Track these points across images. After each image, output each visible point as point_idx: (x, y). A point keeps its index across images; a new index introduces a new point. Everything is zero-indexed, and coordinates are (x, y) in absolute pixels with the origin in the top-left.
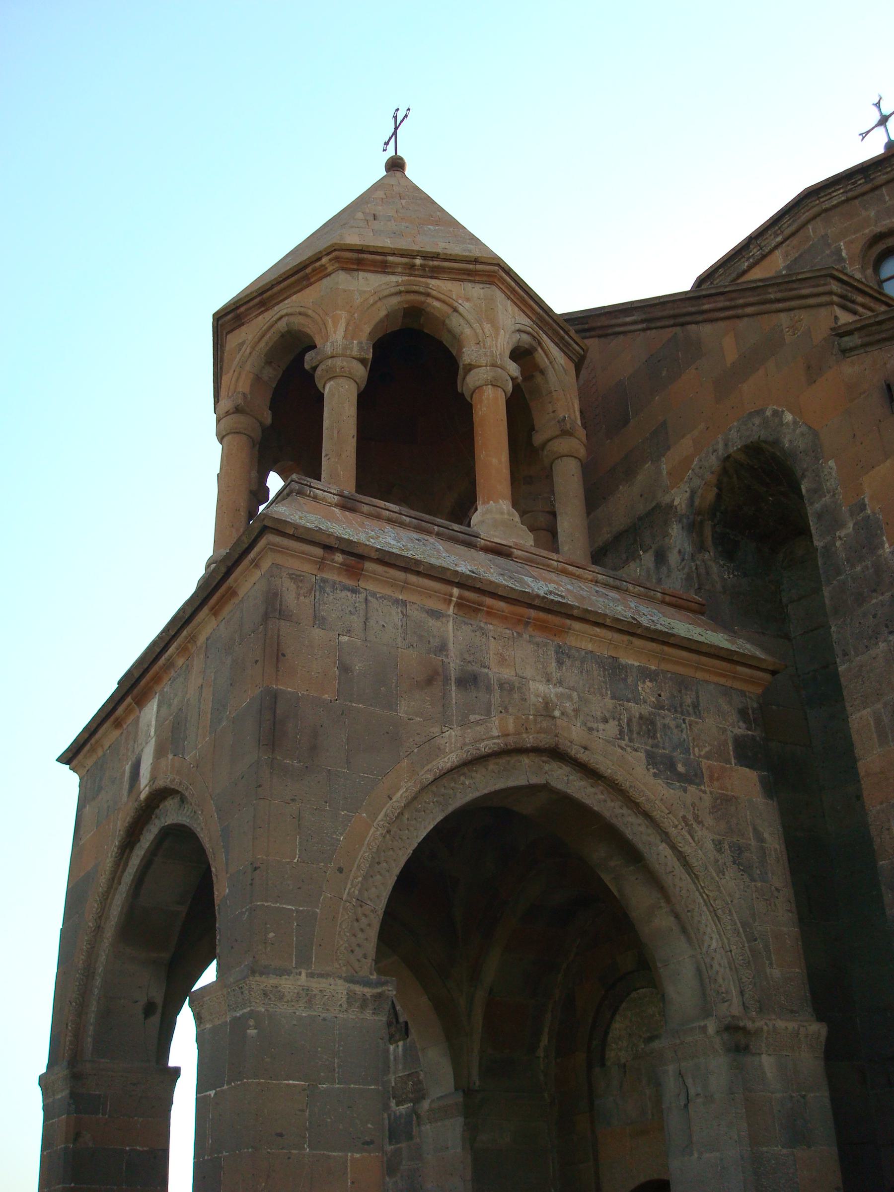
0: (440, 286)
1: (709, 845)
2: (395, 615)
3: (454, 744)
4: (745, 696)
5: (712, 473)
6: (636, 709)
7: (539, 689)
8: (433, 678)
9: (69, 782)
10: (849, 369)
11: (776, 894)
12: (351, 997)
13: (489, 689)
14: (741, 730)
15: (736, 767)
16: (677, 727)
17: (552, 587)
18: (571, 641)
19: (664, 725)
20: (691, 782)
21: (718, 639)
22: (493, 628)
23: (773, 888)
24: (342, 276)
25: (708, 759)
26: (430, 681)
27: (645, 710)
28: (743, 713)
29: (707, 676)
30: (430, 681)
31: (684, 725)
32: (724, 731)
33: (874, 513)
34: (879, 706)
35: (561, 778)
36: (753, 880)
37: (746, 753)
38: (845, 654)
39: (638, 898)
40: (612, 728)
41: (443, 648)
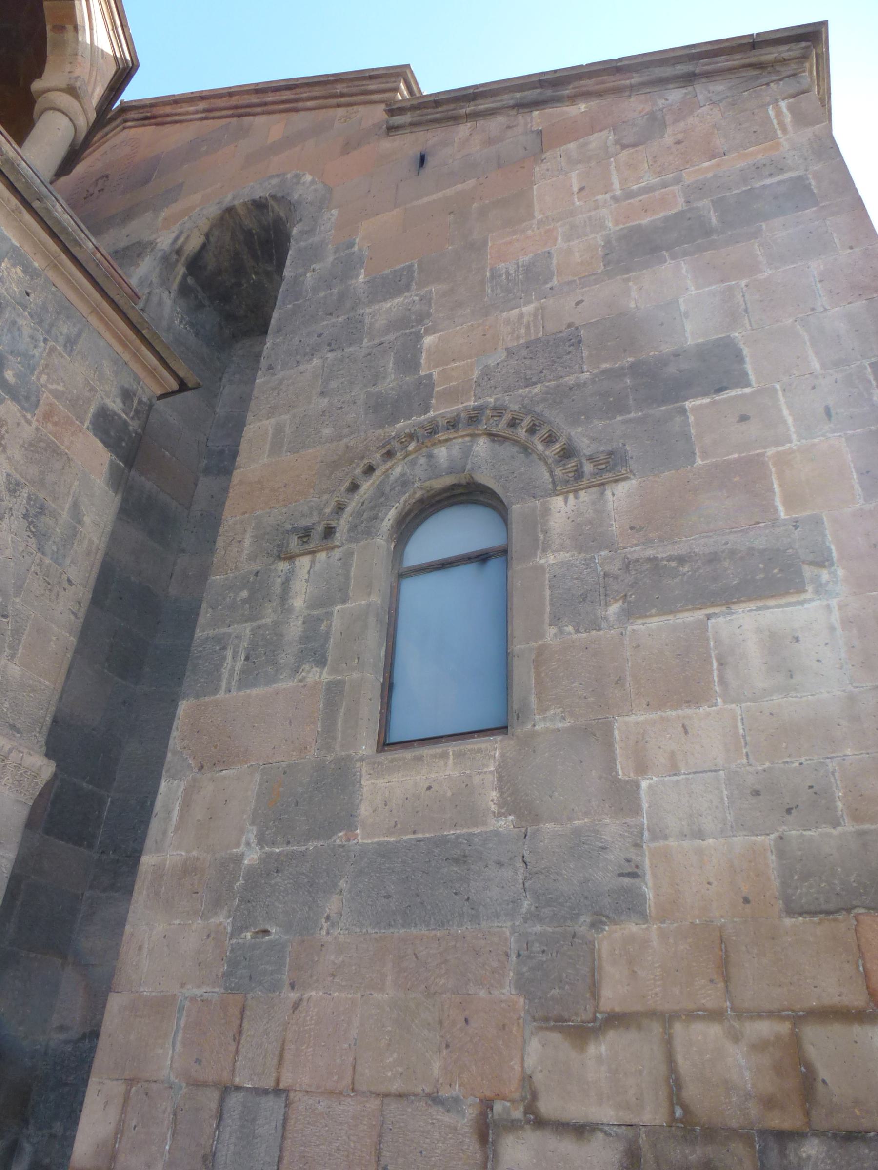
4: (139, 384)
5: (208, 219)
10: (387, 145)
11: (65, 584)
14: (115, 405)
15: (88, 432)
16: (32, 337)
19: (14, 323)
20: (15, 398)
23: (64, 577)
25: (56, 397)
28: (127, 395)
29: (102, 329)
31: (42, 344)
32: (92, 389)
33: (360, 250)
34: (286, 417)
36: (41, 549)
38: (270, 368)
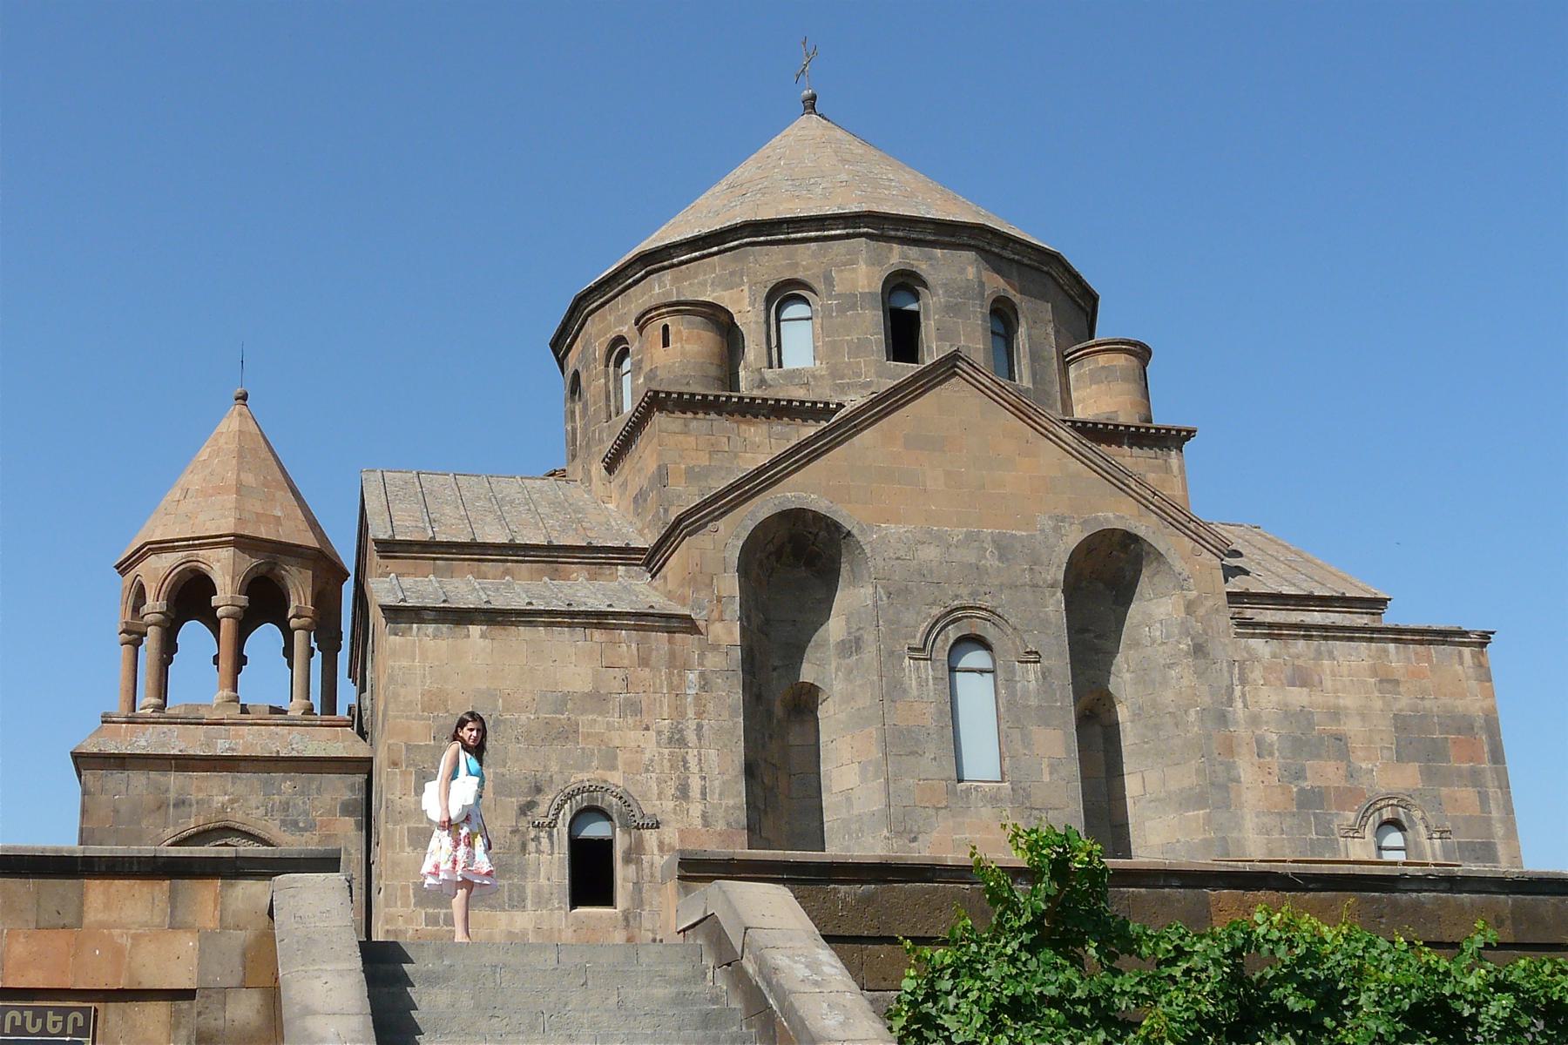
27: (283, 798)
28: (352, 788)
37: (347, 809)
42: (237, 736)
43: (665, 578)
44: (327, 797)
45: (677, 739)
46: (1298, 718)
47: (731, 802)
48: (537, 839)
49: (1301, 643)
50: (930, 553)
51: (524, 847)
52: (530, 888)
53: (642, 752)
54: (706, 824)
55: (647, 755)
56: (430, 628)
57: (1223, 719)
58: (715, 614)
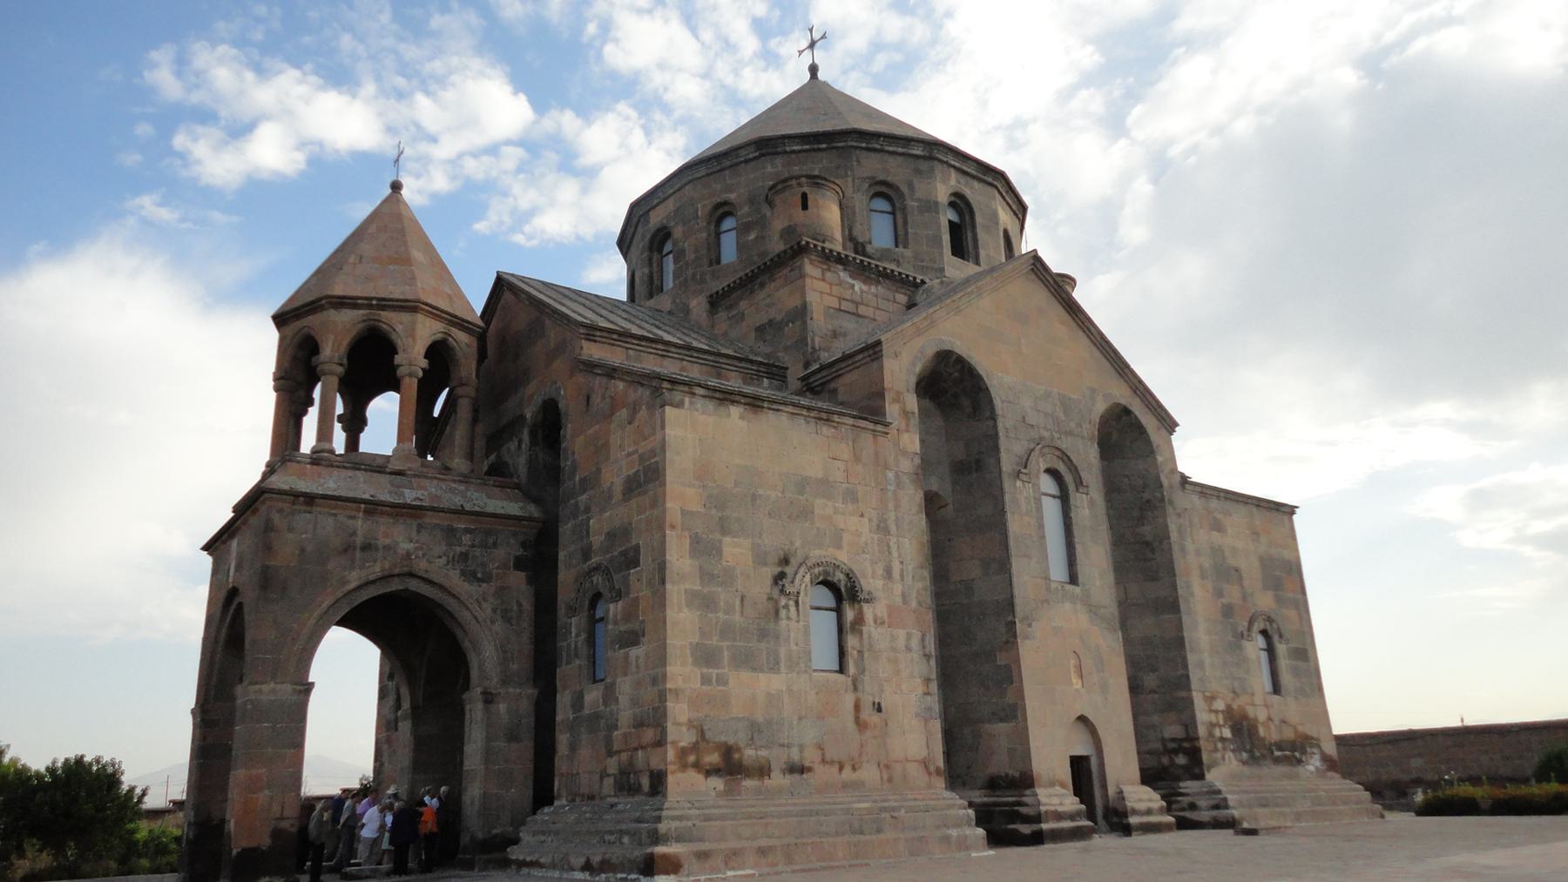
0: (386, 316)
1: (489, 611)
2: (331, 520)
3: (354, 578)
6: (458, 549)
7: (405, 546)
8: (347, 549)
9: (207, 560)
12: (295, 691)
13: (377, 550)
17: (419, 494)
18: (427, 520)
21: (513, 508)
22: (381, 520)
24: (332, 312)
26: (345, 550)
27: (463, 549)
28: (523, 545)
30: (345, 550)
35: (414, 585)
37: (519, 564)
39: (459, 633)
40: (444, 560)
41: (354, 533)
42: (421, 488)
43: (835, 391)
44: (501, 553)
45: (882, 528)
46: (1217, 551)
47: (920, 585)
48: (786, 607)
49: (1214, 503)
50: (1027, 402)
51: (777, 612)
52: (783, 652)
53: (859, 535)
54: (905, 602)
55: (863, 539)
56: (700, 403)
57: (1183, 550)
58: (903, 426)
